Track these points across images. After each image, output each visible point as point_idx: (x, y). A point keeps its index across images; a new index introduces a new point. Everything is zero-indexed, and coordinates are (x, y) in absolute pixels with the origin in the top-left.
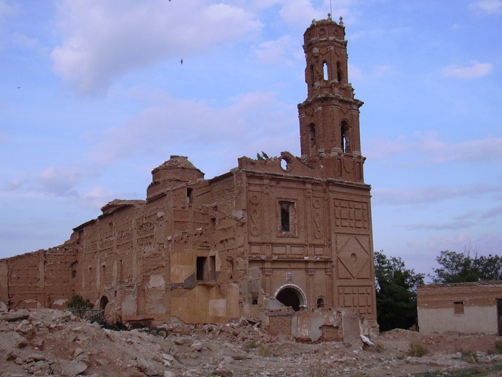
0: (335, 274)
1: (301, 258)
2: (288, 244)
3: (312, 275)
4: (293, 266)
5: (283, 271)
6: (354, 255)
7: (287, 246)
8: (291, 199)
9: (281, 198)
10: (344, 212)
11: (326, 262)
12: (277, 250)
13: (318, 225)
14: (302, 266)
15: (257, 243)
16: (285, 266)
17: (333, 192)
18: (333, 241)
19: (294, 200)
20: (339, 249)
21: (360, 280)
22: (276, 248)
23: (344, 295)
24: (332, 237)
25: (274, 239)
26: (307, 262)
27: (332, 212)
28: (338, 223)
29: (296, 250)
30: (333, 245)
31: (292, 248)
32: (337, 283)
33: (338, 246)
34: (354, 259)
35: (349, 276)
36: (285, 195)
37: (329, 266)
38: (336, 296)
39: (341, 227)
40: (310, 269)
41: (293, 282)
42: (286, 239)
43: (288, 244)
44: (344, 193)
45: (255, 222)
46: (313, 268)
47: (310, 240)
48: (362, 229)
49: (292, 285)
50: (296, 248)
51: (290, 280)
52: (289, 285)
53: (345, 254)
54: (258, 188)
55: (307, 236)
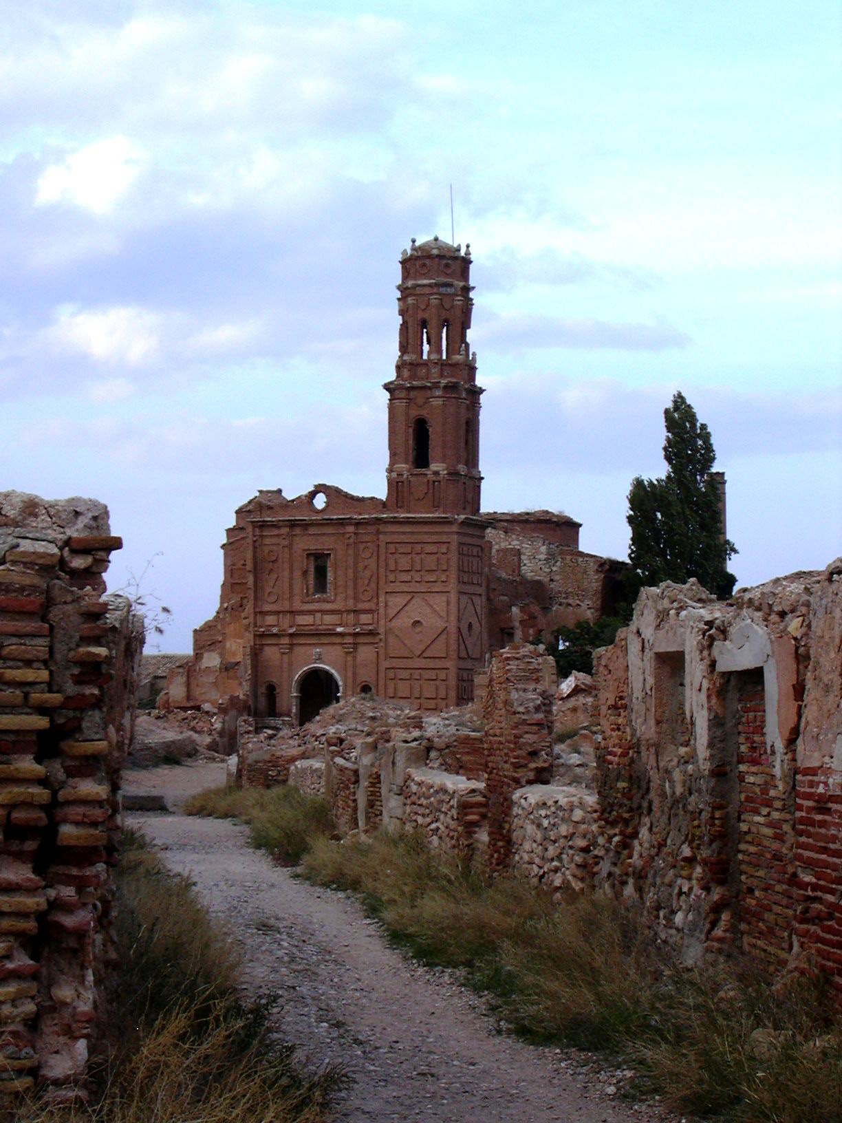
4: (325, 640)
5: (308, 648)
6: (417, 623)
10: (404, 562)
11: (372, 633)
12: (301, 620)
14: (337, 640)
17: (385, 533)
18: (382, 605)
25: (297, 605)
26: (341, 635)
27: (382, 564)
29: (328, 619)
30: (382, 611)
32: (387, 664)
36: (315, 545)
44: (404, 533)
48: (439, 584)
51: (319, 659)
54: (275, 540)
55: (346, 600)
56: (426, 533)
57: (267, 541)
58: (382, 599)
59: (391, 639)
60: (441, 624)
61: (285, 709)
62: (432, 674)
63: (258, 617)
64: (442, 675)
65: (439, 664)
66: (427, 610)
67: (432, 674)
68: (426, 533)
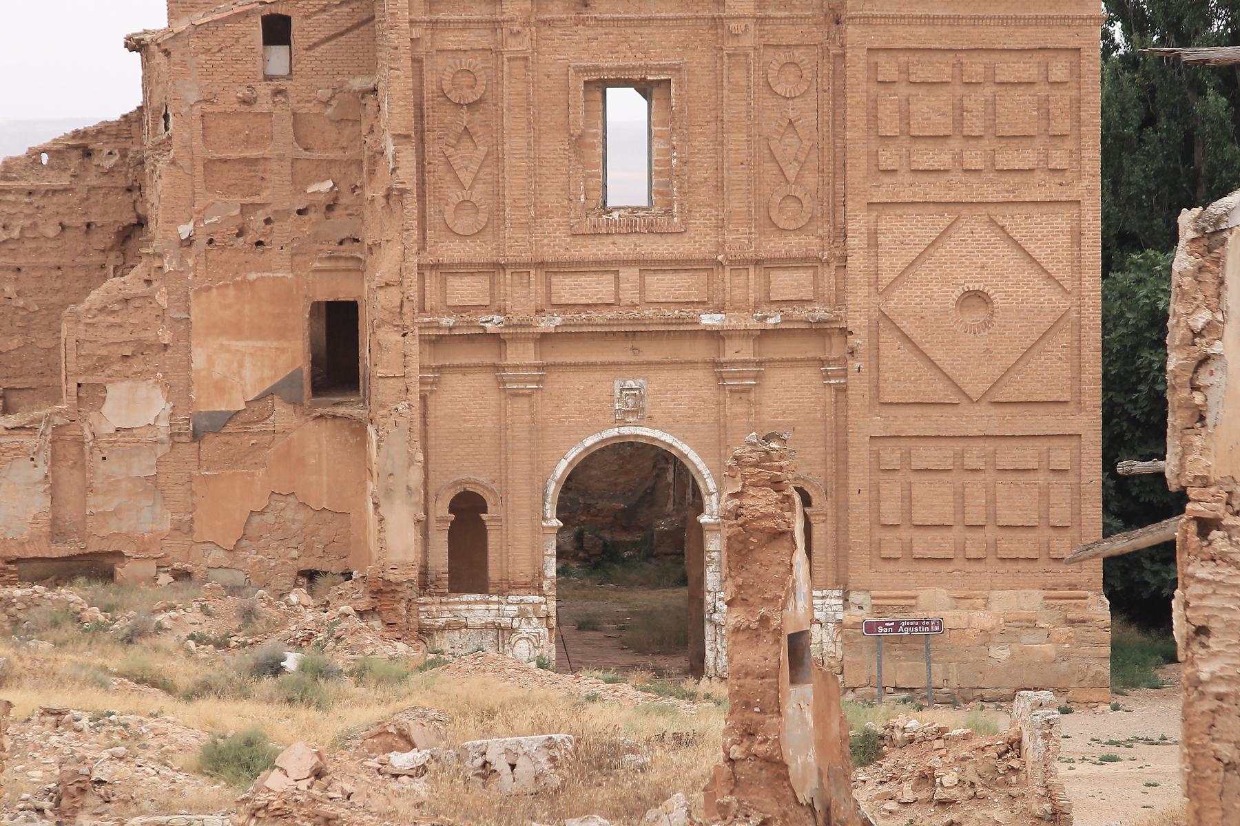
0: (859, 388)
1: (680, 321)
2: (626, 263)
3: (746, 390)
4: (651, 352)
7: (624, 273)
8: (647, 68)
9: (597, 69)
10: (930, 111)
11: (819, 331)
12: (568, 288)
13: (791, 173)
14: (701, 351)
15: (471, 264)
16: (619, 353)
18: (856, 242)
19: (662, 69)
20: (887, 277)
21: (1009, 410)
22: (568, 280)
23: (913, 478)
24: (851, 226)
26: (716, 336)
27: (856, 115)
28: (889, 159)
30: (856, 261)
31: (650, 278)
32: (877, 424)
33: (884, 262)
34: (977, 316)
35: (941, 391)
37: (836, 350)
38: (858, 478)
39: (910, 178)
40: (732, 363)
41: (651, 422)
42: (620, 240)
43: (626, 263)
44: (930, 20)
45: (466, 177)
46: (746, 363)
47: (739, 239)
48: (1039, 176)
49: (642, 431)
50: (668, 277)
52: (625, 430)
53: (928, 296)
54: (473, 38)
55: (721, 226)
56: (1003, 21)
57: (450, 40)
58: (858, 225)
59: (891, 346)
60: (1053, 301)
61: (522, 570)
62: (1025, 455)
63: (431, 279)
64: (1061, 457)
65: (1046, 422)
66: (1006, 256)
67: (1025, 455)
68: (1003, 21)
